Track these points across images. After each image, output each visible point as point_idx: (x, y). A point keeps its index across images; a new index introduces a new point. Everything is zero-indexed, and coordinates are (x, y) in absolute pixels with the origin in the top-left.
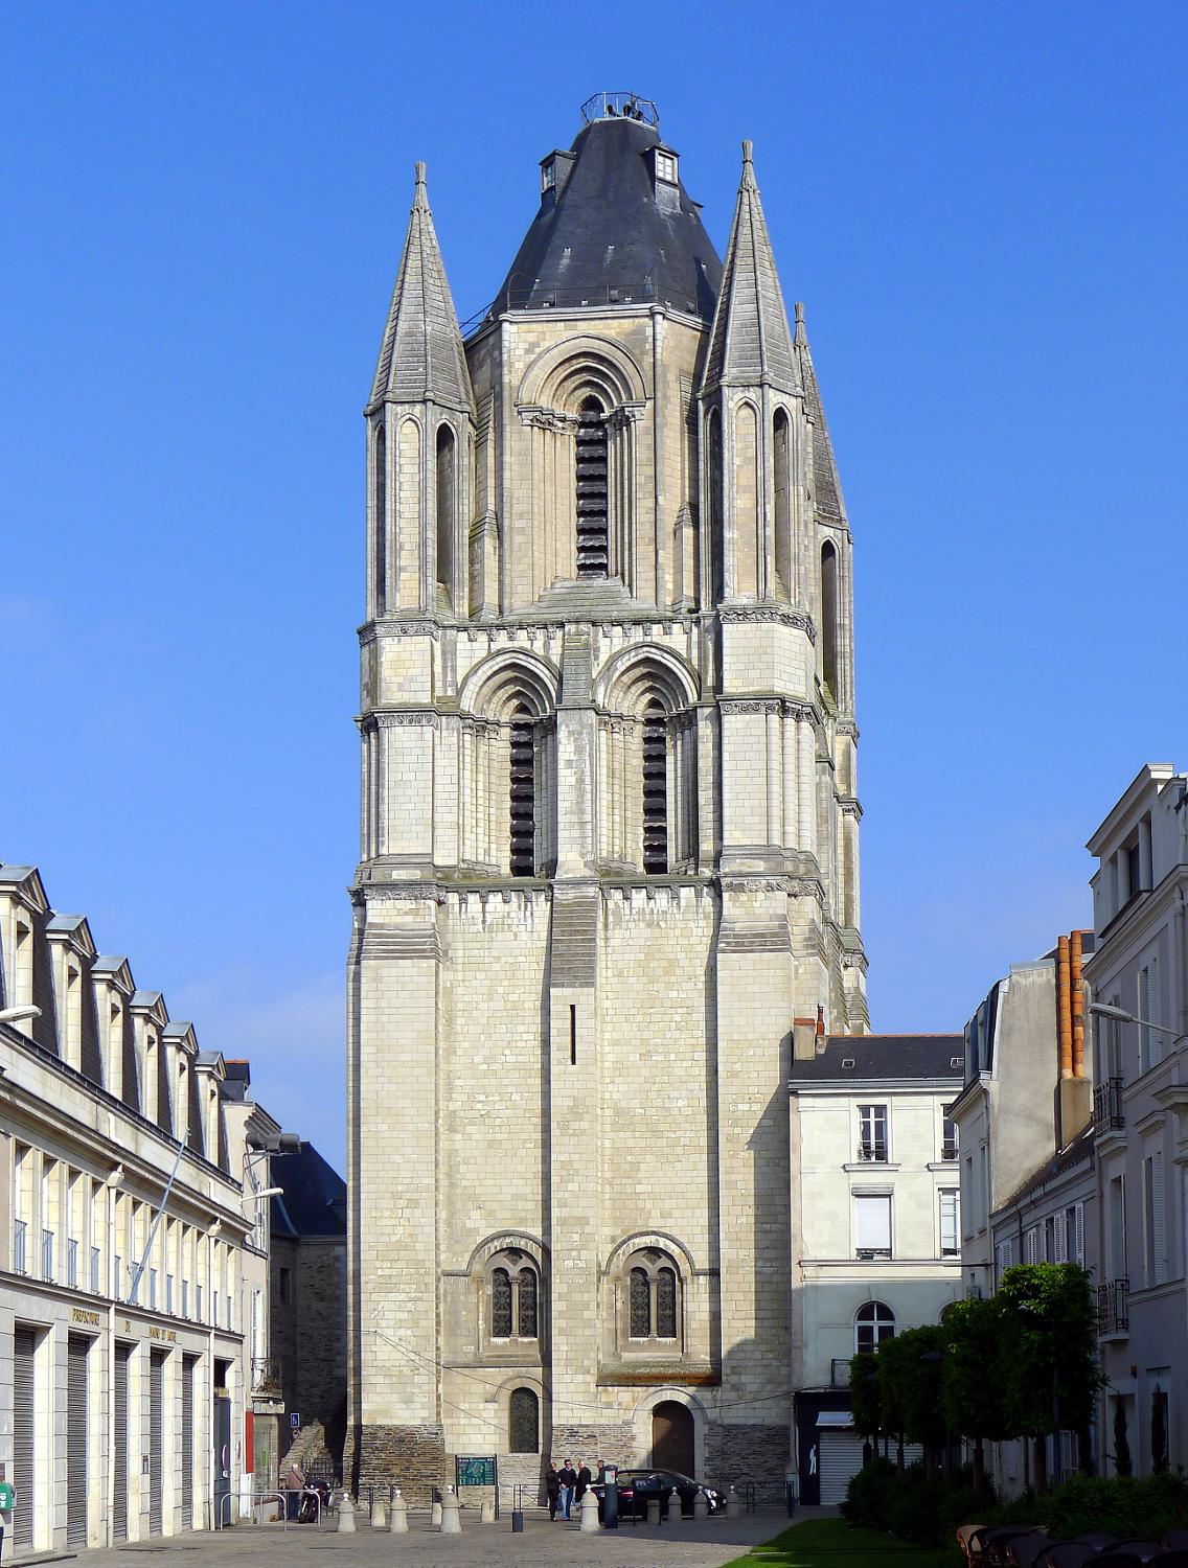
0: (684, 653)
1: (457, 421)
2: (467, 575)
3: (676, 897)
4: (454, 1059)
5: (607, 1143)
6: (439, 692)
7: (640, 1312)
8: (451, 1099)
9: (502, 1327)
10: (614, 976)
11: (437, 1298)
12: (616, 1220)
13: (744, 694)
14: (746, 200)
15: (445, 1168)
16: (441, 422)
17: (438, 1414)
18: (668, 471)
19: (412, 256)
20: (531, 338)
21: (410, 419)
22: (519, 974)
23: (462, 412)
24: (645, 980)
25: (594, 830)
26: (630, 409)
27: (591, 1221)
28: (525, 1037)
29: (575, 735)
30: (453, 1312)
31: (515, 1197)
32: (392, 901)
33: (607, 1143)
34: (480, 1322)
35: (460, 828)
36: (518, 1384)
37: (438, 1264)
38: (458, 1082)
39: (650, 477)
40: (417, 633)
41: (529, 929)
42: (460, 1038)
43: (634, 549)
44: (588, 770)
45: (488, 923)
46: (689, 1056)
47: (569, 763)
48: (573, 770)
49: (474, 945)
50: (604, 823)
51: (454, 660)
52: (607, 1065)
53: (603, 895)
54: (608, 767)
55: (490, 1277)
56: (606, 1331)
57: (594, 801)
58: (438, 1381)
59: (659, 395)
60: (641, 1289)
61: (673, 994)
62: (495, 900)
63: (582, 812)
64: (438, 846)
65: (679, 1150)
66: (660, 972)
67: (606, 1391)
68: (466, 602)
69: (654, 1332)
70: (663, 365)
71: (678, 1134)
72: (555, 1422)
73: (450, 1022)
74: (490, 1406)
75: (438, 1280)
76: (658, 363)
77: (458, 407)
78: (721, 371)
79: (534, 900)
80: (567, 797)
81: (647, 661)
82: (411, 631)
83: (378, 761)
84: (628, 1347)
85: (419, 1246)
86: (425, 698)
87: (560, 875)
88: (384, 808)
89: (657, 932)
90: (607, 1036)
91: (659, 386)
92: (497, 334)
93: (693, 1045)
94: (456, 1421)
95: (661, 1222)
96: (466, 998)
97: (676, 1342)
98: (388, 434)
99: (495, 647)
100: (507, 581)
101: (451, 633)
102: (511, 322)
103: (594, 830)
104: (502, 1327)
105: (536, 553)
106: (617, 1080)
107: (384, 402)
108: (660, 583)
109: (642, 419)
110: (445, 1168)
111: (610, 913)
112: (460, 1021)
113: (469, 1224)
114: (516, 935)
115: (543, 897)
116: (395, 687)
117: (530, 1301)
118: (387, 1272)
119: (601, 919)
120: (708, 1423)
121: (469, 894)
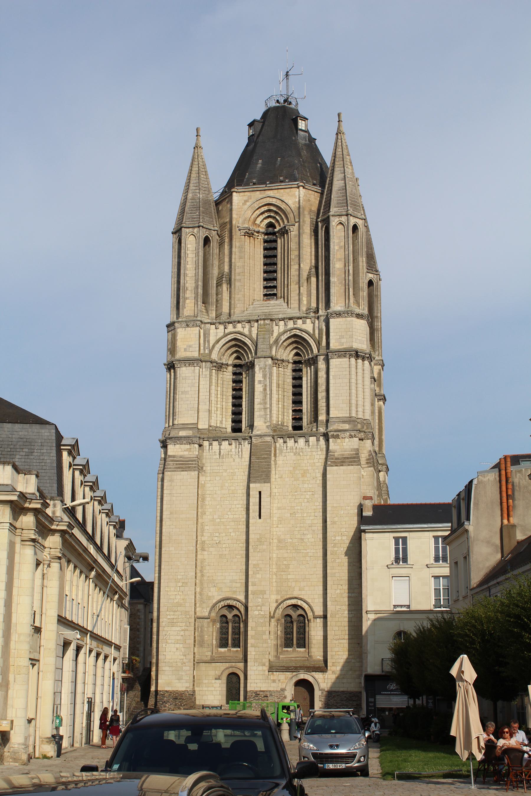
2: (215, 300)
3: (307, 441)
4: (204, 517)
5: (275, 556)
6: (202, 351)
7: (288, 636)
8: (203, 536)
9: (223, 643)
10: (279, 478)
11: (195, 629)
12: (278, 592)
13: (339, 349)
14: (339, 137)
15: (198, 567)
17: (194, 685)
18: (304, 253)
19: (194, 166)
20: (245, 198)
21: (192, 234)
22: (235, 477)
23: (214, 231)
24: (293, 479)
25: (271, 412)
27: (268, 592)
28: (237, 506)
29: (263, 369)
30: (202, 636)
31: (232, 581)
33: (275, 556)
34: (214, 641)
35: (210, 411)
36: (231, 670)
37: (195, 613)
40: (193, 326)
41: (240, 457)
42: (208, 507)
43: (289, 287)
45: (222, 454)
46: (313, 514)
47: (260, 382)
49: (215, 464)
50: (274, 408)
51: (209, 337)
52: (275, 519)
55: (218, 619)
56: (273, 645)
57: (271, 399)
58: (194, 669)
59: (301, 220)
60: (289, 625)
61: (306, 486)
62: (225, 444)
64: (200, 420)
65: (308, 559)
66: (300, 475)
67: (273, 674)
68: (214, 312)
69: (295, 646)
70: (303, 208)
71: (308, 551)
72: (249, 689)
73: (203, 499)
74: (217, 681)
75: (195, 621)
76: (301, 207)
77: (213, 228)
78: (329, 209)
79: (243, 443)
80: (259, 397)
81: (295, 336)
82: (191, 325)
83: (174, 383)
84: (282, 652)
85: (187, 605)
86: (196, 355)
87: (255, 432)
88: (177, 403)
89: (299, 457)
90: (275, 505)
92: (230, 197)
94: (201, 689)
95: (299, 593)
96: (211, 489)
97: (305, 651)
98: (183, 241)
99: (227, 331)
100: (233, 302)
101: (208, 326)
102: (236, 192)
103: (271, 412)
104: (223, 643)
105: (246, 290)
106: (279, 526)
107: (181, 228)
108: (301, 301)
109: (294, 231)
110: (198, 567)
112: (208, 499)
113: (210, 594)
114: (234, 460)
115: (247, 442)
116: (183, 350)
117: (237, 630)
118: (172, 617)
119: (273, 452)
120: (321, 690)
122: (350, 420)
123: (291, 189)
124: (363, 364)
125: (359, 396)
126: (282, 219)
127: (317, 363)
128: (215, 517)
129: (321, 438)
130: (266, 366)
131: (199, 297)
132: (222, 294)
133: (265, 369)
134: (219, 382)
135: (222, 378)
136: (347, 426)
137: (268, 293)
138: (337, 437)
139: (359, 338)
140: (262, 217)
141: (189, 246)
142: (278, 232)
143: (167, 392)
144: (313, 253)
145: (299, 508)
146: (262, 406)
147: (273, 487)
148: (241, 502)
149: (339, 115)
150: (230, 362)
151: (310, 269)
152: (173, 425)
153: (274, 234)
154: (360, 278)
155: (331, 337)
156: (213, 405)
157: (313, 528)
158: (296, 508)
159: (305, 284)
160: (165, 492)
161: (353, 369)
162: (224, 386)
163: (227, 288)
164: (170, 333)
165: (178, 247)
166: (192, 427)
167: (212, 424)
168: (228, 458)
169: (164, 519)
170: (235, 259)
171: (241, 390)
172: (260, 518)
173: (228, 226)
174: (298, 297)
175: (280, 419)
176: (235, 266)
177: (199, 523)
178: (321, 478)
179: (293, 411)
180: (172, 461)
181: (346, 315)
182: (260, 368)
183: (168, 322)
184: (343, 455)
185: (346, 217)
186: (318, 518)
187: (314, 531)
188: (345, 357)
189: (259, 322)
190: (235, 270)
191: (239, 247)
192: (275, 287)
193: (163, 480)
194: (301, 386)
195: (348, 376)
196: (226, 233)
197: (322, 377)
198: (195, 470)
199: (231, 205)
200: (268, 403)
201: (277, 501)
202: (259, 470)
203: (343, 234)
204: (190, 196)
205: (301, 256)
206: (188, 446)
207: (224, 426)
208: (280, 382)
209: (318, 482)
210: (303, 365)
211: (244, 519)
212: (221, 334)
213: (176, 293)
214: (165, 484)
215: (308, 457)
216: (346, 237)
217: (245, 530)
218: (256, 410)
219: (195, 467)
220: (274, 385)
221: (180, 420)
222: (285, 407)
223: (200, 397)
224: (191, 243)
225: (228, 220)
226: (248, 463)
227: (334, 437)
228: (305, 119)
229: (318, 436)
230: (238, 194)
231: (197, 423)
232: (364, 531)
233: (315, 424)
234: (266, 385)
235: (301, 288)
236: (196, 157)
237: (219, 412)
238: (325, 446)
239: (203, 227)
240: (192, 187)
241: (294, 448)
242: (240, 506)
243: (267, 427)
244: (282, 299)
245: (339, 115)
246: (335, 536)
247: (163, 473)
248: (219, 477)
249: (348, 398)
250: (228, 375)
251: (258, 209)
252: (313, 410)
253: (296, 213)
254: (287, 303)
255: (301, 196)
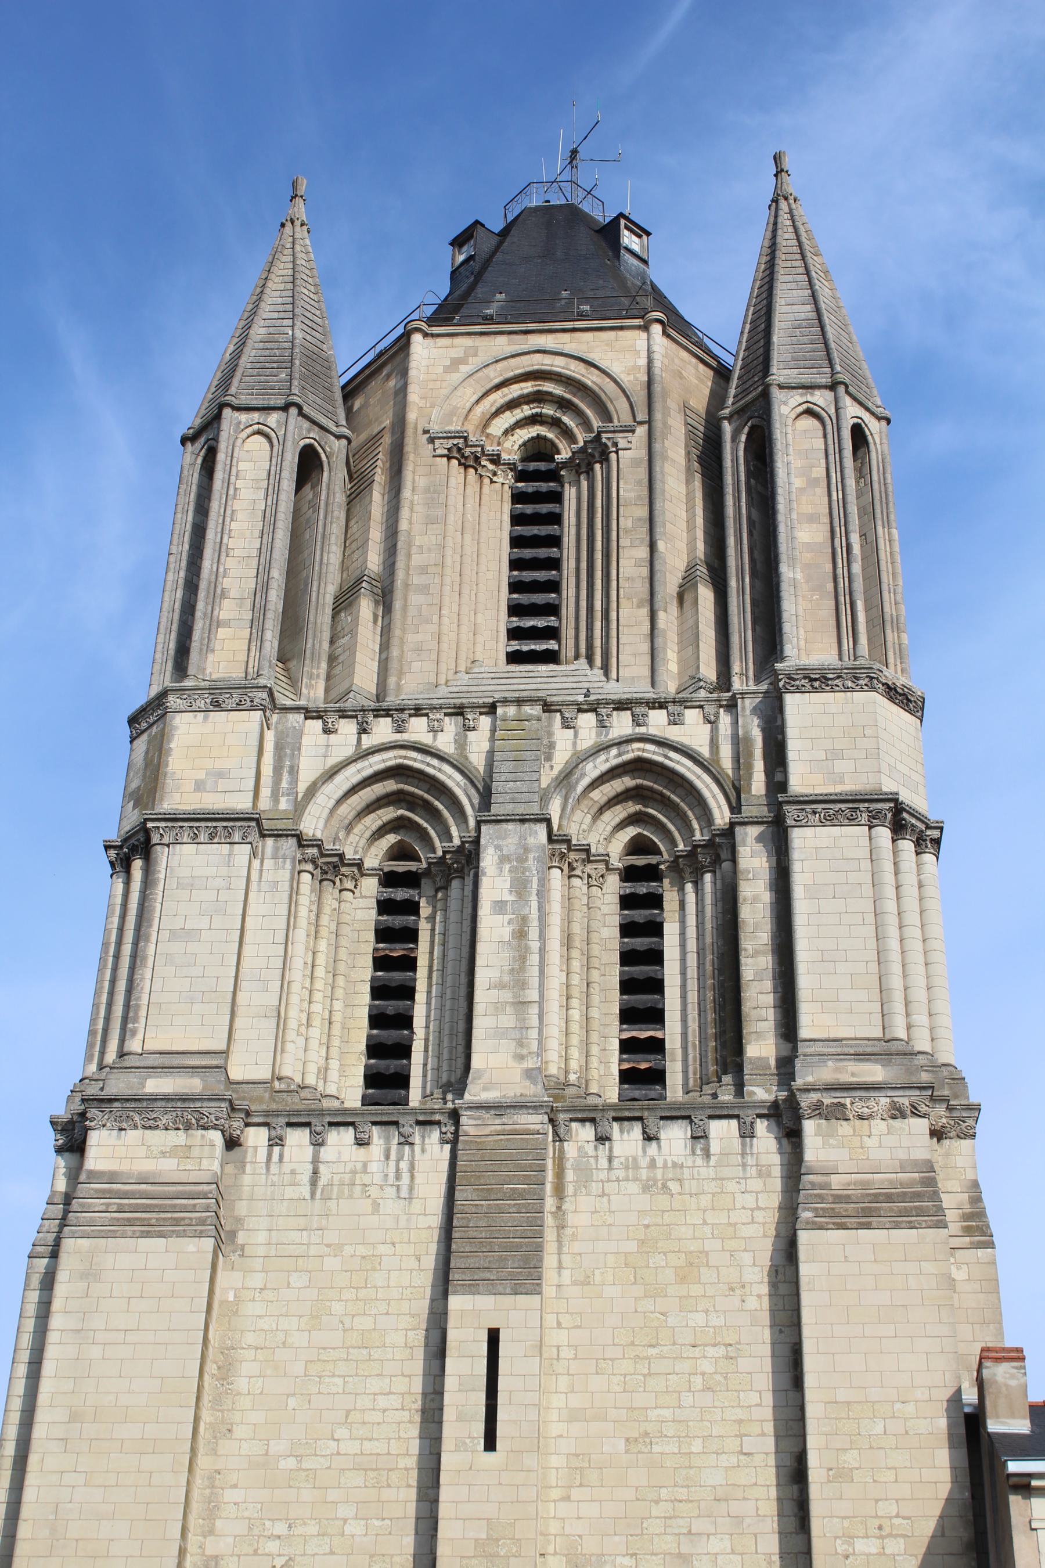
0: (705, 751)
1: (331, 448)
3: (700, 1137)
4: (226, 1446)
6: (264, 804)
8: (211, 1532)
10: (575, 1283)
16: (307, 441)
20: (455, 353)
21: (259, 432)
23: (338, 437)
26: (610, 435)
28: (382, 1402)
32: (140, 1132)
35: (281, 1021)
38: (230, 1495)
39: (640, 519)
40: (239, 707)
41: (404, 1193)
42: (245, 1402)
43: (613, 615)
44: (534, 914)
45: (323, 1181)
46: (732, 1444)
47: (500, 907)
48: (507, 918)
52: (555, 1461)
53: (556, 1133)
54: (563, 931)
59: (658, 416)
61: (699, 1319)
62: (340, 1140)
63: (523, 985)
64: (235, 1047)
66: (669, 1275)
68: (321, 685)
73: (226, 1372)
76: (657, 378)
77: (334, 429)
79: (417, 1139)
81: (639, 766)
86: (242, 803)
87: (475, 1093)
89: (663, 1201)
90: (557, 1401)
91: (658, 406)
92: (398, 359)
93: (740, 1422)
99: (367, 741)
100: (395, 652)
102: (426, 335)
105: (445, 620)
106: (575, 1494)
107: (222, 406)
108: (659, 656)
109: (630, 453)
111: (568, 1165)
112: (247, 1368)
114: (376, 1207)
115: (435, 1135)
116: (190, 786)
119: (550, 1176)
121: (289, 1130)
122: (888, 1050)
123: (621, 333)
124: (919, 865)
125: (911, 969)
126: (586, 424)
127: (734, 860)
128: (277, 1447)
129: (761, 1127)
130: (527, 850)
131: (270, 615)
132: (353, 633)
133: (522, 859)
134: (325, 920)
135: (338, 911)
136: (875, 1072)
137: (525, 648)
138: (837, 1113)
139: (900, 767)
140: (508, 418)
141: (242, 466)
142: (564, 465)
143: (105, 945)
144: (700, 521)
145: (667, 1413)
146: (507, 996)
147: (550, 1320)
148: (400, 1385)
149: (777, 158)
150: (372, 861)
151: (691, 569)
152: (121, 1054)
153: (552, 475)
154: (885, 587)
155: (791, 755)
156: (294, 999)
157: (735, 1507)
158: (653, 1414)
159: (673, 608)
160: (56, 1322)
161: (888, 866)
162: (343, 941)
163: (375, 616)
164: (142, 743)
165: (200, 486)
166: (204, 1063)
167: (286, 1072)
168: (351, 1197)
169: (36, 1445)
170: (411, 524)
171: (409, 964)
172: (490, 1444)
173: (387, 440)
174: (646, 647)
175: (574, 1065)
176: (409, 544)
177: (198, 1473)
178: (765, 1289)
179: (627, 1046)
180: (102, 1195)
181: (850, 684)
182: (503, 859)
183: (140, 701)
184: (865, 1185)
185: (829, 395)
186: (758, 1459)
187: (739, 1519)
188: (852, 821)
189: (500, 711)
190: (409, 556)
191: (427, 490)
192: (552, 633)
193: (48, 1282)
194: (656, 957)
195: (868, 891)
196: (380, 456)
197: (756, 899)
198: (200, 1235)
199: (404, 373)
200: (534, 982)
201: (563, 1383)
202: (484, 1239)
203: (820, 443)
204: (258, 331)
205: (658, 519)
206: (178, 1138)
207: (332, 1089)
208: (577, 929)
209: (752, 1303)
210: (666, 882)
211: (411, 1462)
212: (349, 751)
213: (176, 616)
214: (61, 1289)
215: (705, 1201)
216: (831, 455)
217: (411, 1509)
218: (479, 1009)
219: (202, 1222)
220: (555, 933)
221: (153, 1035)
222: (595, 1025)
223: (245, 963)
224: (252, 463)
225: (387, 423)
226: (435, 1220)
227: (819, 1111)
228: (641, 232)
229: (748, 1115)
230: (429, 341)
231: (225, 1053)
232: (1024, 1486)
233: (727, 1079)
234: (524, 920)
235: (661, 615)
236: (289, 245)
237: (315, 1033)
238: (776, 1159)
239: (301, 413)
240: (266, 309)
241: (644, 1162)
242: (395, 1401)
243: (529, 1074)
244: (583, 662)
245: (777, 158)
246: (849, 1538)
247: (54, 1255)
248: (305, 1278)
249: (874, 967)
250: (360, 907)
251: (498, 387)
252: (711, 1031)
253: (639, 398)
254: (606, 668)
255: (655, 348)
